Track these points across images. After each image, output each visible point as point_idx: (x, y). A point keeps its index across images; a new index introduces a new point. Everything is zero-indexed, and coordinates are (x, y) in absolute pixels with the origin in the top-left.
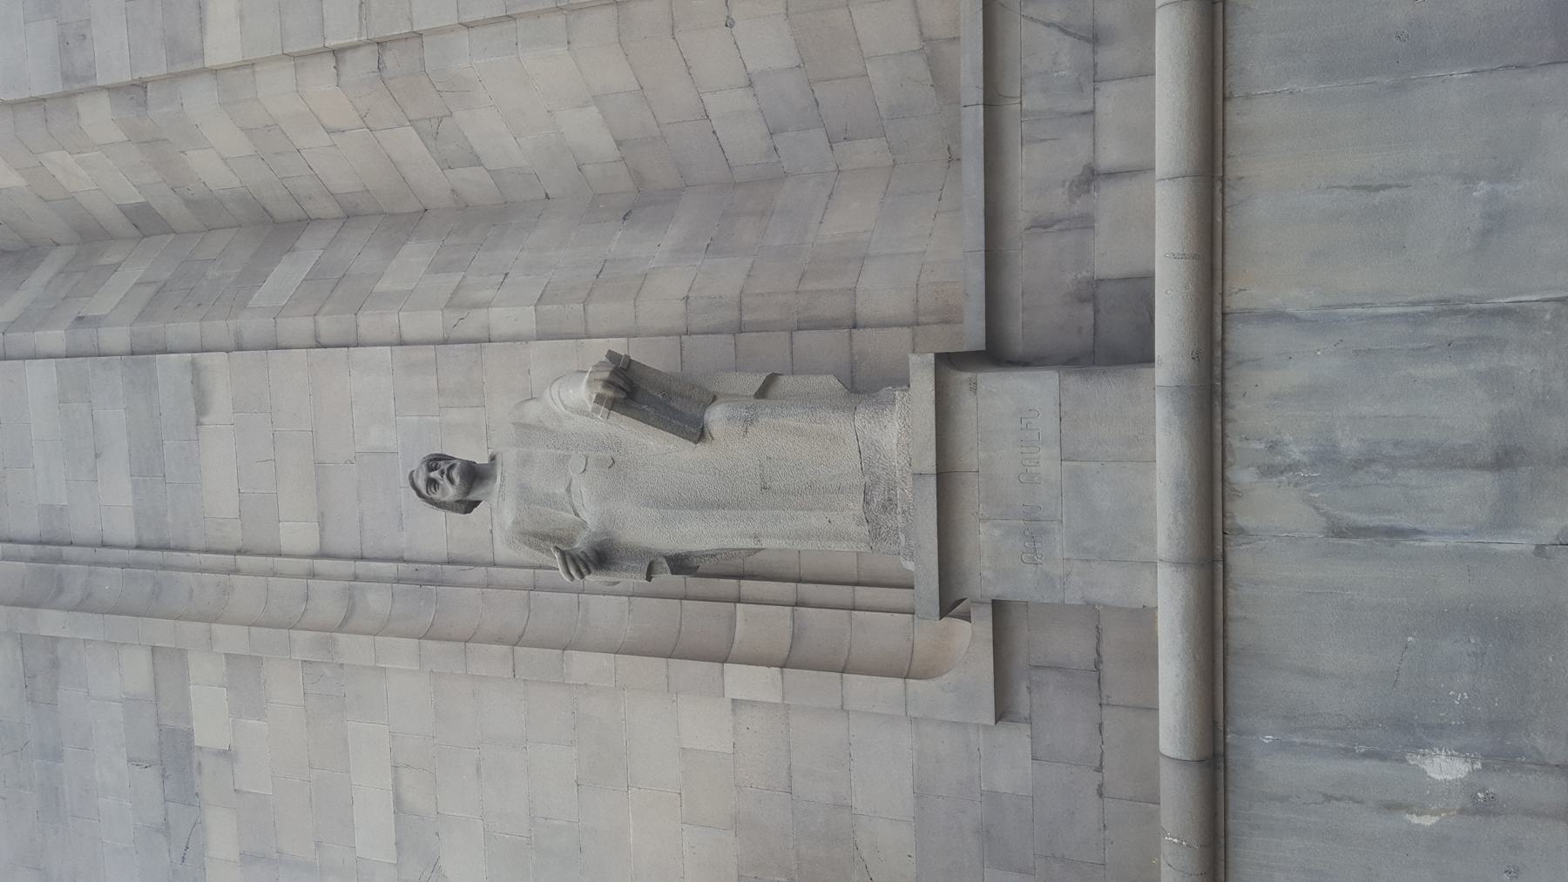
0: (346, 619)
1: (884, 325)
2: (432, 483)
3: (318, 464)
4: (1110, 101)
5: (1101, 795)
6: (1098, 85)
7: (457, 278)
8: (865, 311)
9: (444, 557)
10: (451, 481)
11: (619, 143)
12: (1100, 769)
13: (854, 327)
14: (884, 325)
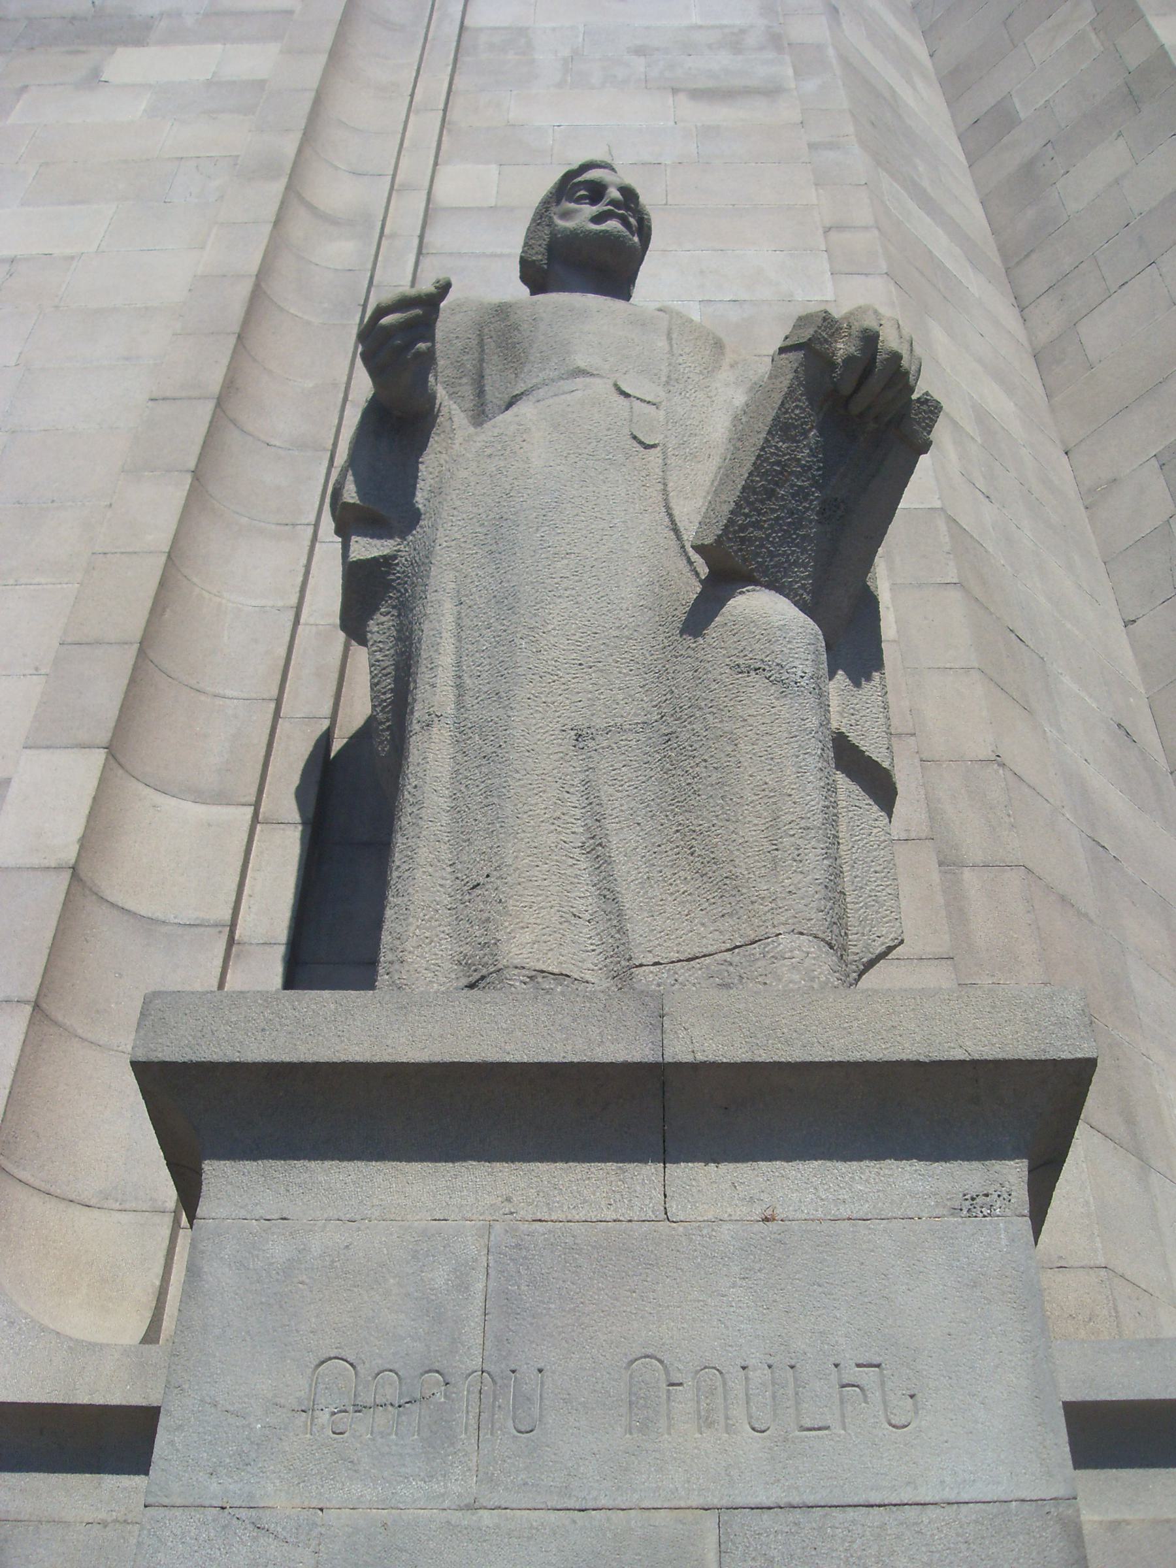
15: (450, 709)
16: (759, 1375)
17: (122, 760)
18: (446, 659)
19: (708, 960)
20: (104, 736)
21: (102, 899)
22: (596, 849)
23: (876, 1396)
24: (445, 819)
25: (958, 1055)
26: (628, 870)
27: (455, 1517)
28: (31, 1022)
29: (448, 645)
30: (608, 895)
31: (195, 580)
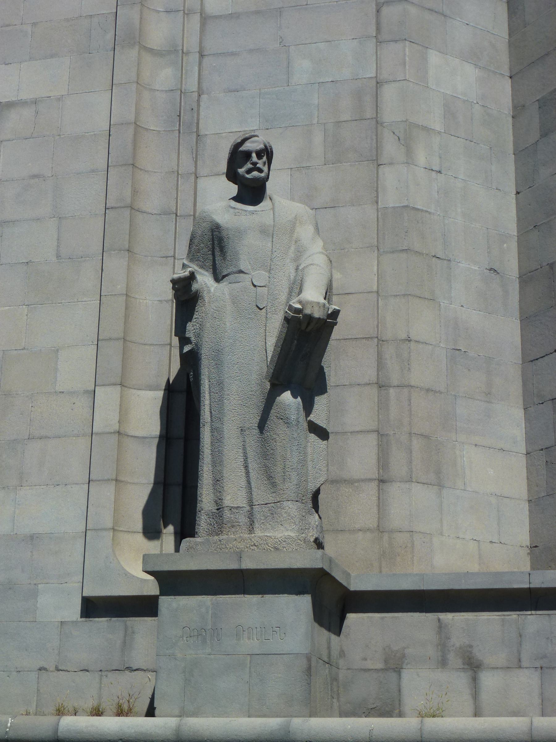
0: (151, 51)
1: (381, 505)
2: (247, 155)
3: (280, 11)
4: (526, 681)
5: (40, 669)
6: (539, 670)
7: (438, 126)
8: (395, 490)
9: (202, 132)
10: (249, 171)
12: (58, 670)
13: (382, 481)
14: (381, 505)
16: (259, 629)
17: (125, 384)
18: (207, 402)
19: (269, 505)
22: (246, 467)
24: (210, 457)
25: (295, 567)
26: (252, 474)
29: (207, 396)
30: (249, 483)
31: (137, 296)
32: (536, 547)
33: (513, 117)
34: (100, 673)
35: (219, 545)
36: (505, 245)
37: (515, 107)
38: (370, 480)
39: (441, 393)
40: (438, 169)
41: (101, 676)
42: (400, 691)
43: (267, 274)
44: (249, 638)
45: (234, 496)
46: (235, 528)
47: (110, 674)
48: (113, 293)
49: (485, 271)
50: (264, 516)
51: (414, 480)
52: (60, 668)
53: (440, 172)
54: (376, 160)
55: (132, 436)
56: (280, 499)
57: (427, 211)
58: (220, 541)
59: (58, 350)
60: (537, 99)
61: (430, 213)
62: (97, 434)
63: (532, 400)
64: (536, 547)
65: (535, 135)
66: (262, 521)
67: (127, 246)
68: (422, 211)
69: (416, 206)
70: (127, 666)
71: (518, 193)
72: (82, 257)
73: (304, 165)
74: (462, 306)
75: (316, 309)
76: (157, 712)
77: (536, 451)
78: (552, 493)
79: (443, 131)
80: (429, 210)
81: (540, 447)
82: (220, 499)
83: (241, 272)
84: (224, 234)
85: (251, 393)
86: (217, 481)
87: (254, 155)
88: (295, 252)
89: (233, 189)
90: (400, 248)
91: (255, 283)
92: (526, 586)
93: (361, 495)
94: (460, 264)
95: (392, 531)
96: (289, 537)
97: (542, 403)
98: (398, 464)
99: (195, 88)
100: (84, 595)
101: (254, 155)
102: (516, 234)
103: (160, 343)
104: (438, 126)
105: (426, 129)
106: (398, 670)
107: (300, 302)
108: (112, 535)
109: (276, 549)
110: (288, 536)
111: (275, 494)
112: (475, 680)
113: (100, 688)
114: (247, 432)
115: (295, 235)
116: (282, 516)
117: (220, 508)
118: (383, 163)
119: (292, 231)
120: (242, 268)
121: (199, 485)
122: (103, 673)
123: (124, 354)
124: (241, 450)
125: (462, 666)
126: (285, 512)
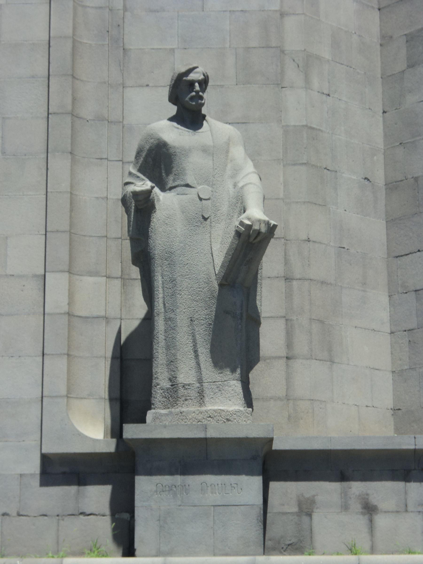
1: (289, 378)
2: (192, 84)
7: (327, 55)
8: (297, 365)
9: (127, 47)
11: (416, 179)
12: (19, 515)
13: (288, 358)
14: (289, 378)
15: (163, 310)
16: (220, 485)
19: (217, 383)
20: (66, 268)
21: (74, 316)
22: (196, 352)
23: (236, 489)
27: (178, 507)
28: (68, 359)
30: (198, 364)
32: (399, 409)
33: (381, 45)
34: (57, 518)
35: (180, 416)
36: (375, 158)
37: (383, 37)
38: (280, 358)
39: (331, 284)
40: (327, 93)
41: (59, 520)
42: (311, 530)
43: (210, 189)
44: (212, 493)
45: (186, 375)
46: (188, 401)
47: (66, 519)
48: (59, 191)
49: (361, 180)
50: (213, 392)
51: (314, 358)
52: (21, 513)
53: (329, 95)
54: (279, 83)
55: (77, 316)
56: (227, 379)
57: (319, 130)
58: (181, 413)
59: (7, 238)
60: (405, 33)
61: (322, 131)
62: (49, 314)
63: (396, 290)
64: (399, 409)
65: (401, 65)
66: (211, 396)
67: (70, 149)
68: (317, 129)
69: (312, 126)
70: (81, 511)
71: (384, 112)
72: (25, 155)
73: (219, 84)
74: (345, 210)
75: (263, 225)
76: (137, 553)
77: (400, 331)
78: (414, 367)
79: (331, 59)
80: (321, 129)
81: (404, 329)
82: (174, 377)
83: (187, 186)
84: (171, 151)
85: (199, 289)
86: (171, 363)
87: (197, 84)
88: (234, 172)
89: (173, 110)
90: (301, 162)
91: (201, 196)
92: (413, 447)
93: (272, 370)
94: (344, 175)
95: (295, 400)
96: (240, 411)
97: (406, 293)
98: (301, 345)
99: (121, 7)
100: (44, 451)
101: (197, 84)
102: (382, 147)
103: (98, 235)
104: (327, 55)
105: (319, 58)
106: (310, 515)
107: (249, 219)
108: (66, 402)
109: (228, 420)
110: (238, 409)
111: (222, 375)
112: (371, 521)
113: (58, 530)
114: (196, 322)
115: (230, 155)
116: (230, 393)
117: (174, 385)
118: (285, 86)
119: (227, 152)
120: (189, 182)
121: (154, 364)
122: (60, 518)
123: (70, 244)
124: (191, 337)
125: (361, 510)
126: (232, 390)
